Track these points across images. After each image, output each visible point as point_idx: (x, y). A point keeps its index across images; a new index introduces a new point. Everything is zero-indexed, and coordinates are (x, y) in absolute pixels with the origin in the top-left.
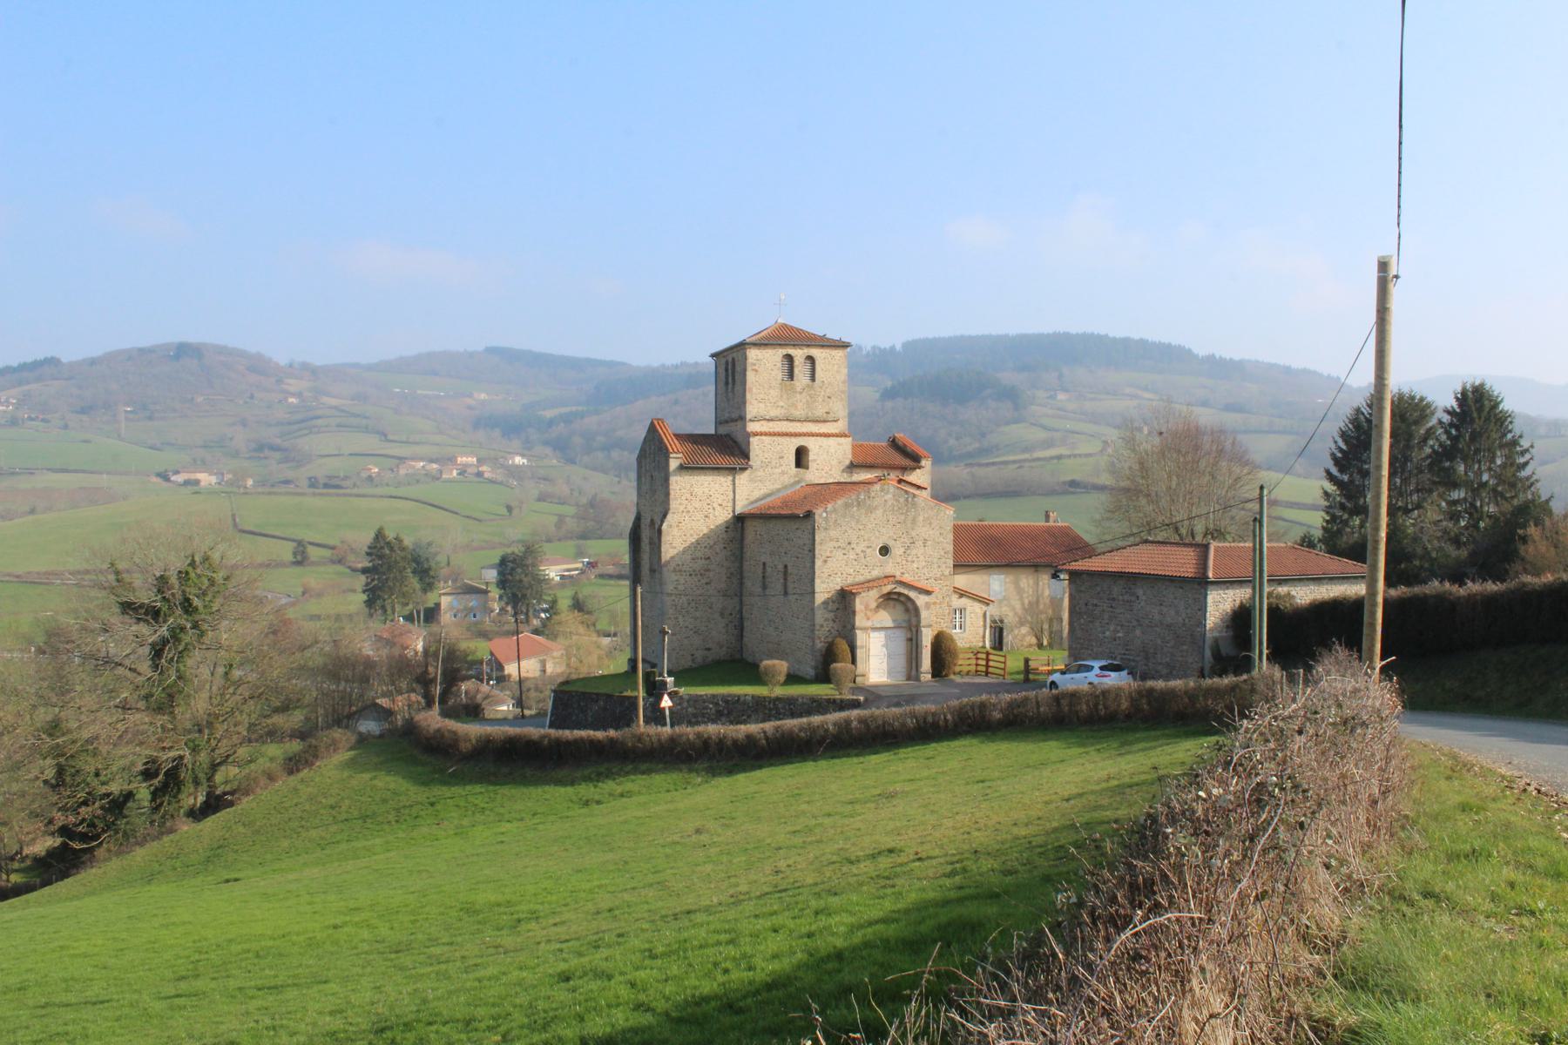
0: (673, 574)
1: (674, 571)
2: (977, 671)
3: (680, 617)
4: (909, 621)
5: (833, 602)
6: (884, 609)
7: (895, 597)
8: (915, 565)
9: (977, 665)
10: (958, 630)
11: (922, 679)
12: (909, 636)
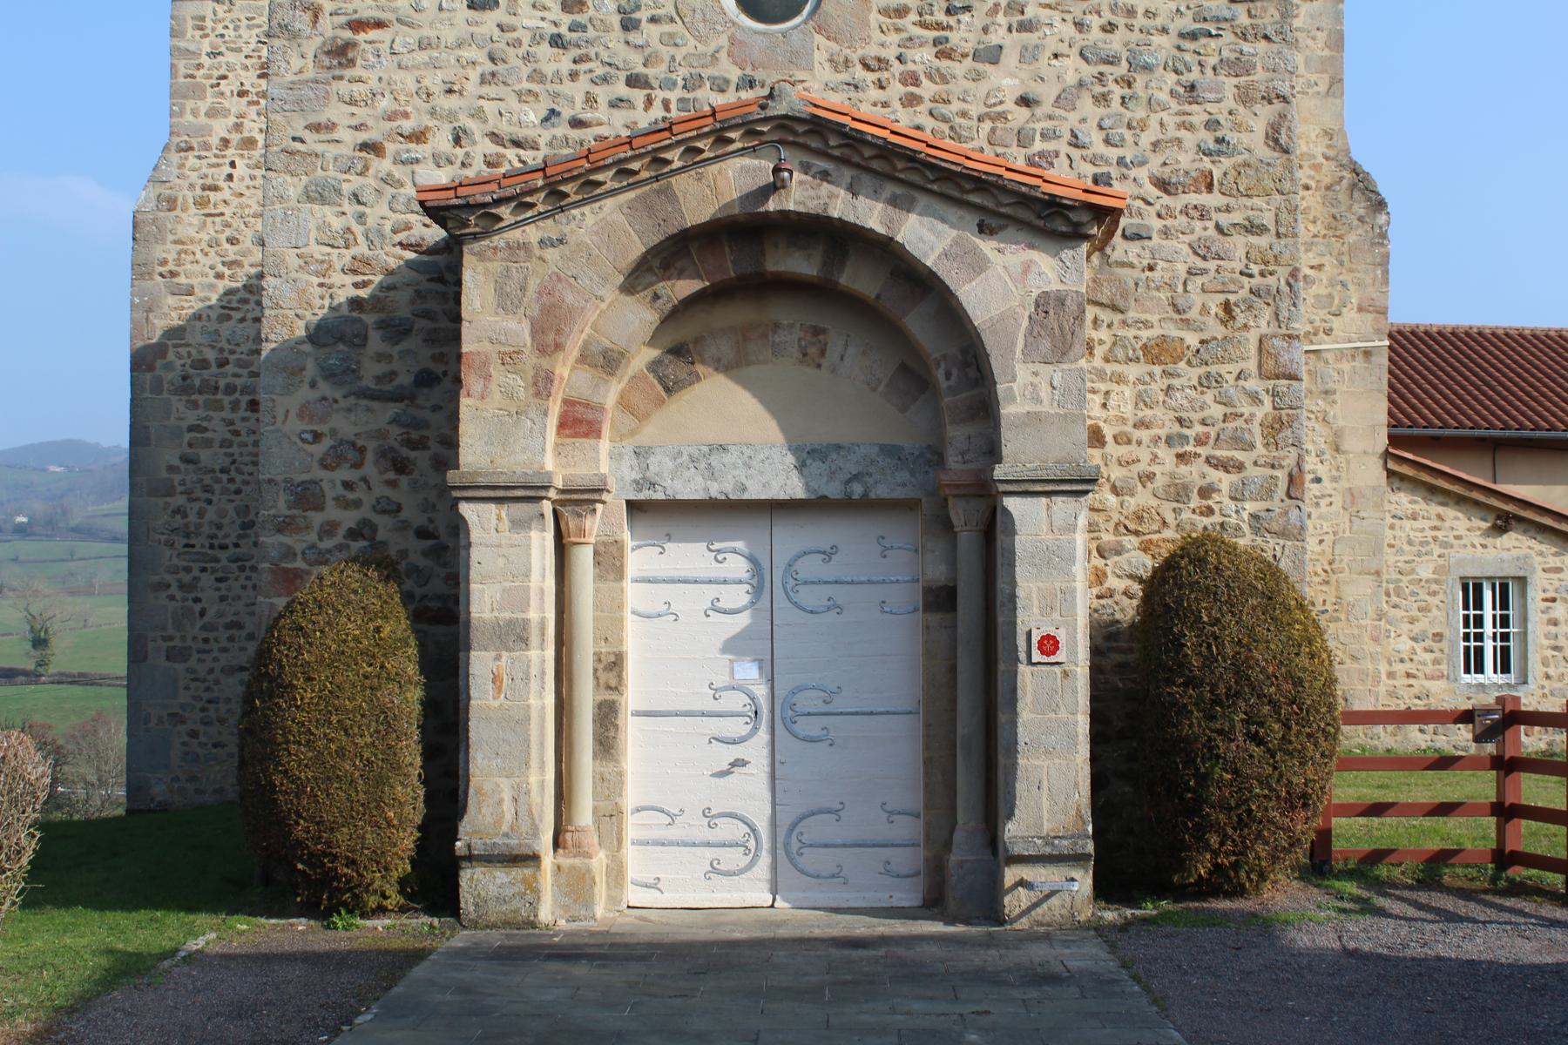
0: (178, 403)
1: (184, 387)
2: (1503, 858)
3: (207, 580)
4: (935, 456)
5: (396, 330)
6: (726, 367)
7: (802, 264)
8: (1007, 81)
9: (1505, 812)
10: (1490, 676)
11: (1015, 902)
12: (937, 573)
